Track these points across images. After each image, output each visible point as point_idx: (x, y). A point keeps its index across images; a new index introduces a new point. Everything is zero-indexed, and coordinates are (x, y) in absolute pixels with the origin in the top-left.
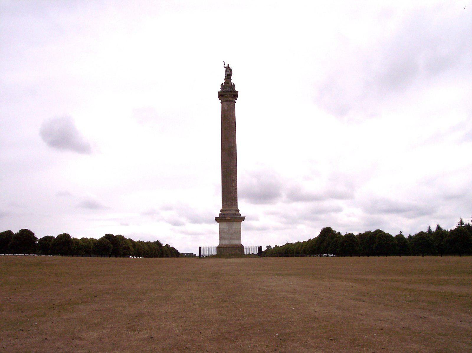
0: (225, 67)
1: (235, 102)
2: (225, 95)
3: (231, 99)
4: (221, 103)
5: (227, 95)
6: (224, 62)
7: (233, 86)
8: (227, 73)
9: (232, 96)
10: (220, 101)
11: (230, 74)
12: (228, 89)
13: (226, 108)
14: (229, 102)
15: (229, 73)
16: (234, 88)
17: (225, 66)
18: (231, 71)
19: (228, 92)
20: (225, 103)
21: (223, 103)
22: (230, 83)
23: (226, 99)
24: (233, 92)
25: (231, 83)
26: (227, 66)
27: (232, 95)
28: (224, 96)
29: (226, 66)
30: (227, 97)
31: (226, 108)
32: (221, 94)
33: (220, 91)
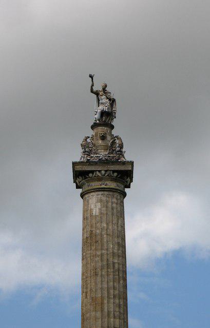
0: (97, 94)
1: (124, 195)
2: (92, 172)
3: (112, 185)
4: (82, 196)
5: (100, 171)
6: (91, 77)
7: (116, 148)
8: (101, 107)
9: (116, 174)
10: (80, 191)
11: (110, 111)
12: (102, 154)
13: (96, 211)
14: (106, 193)
15: (106, 109)
16: (121, 153)
17: (95, 89)
18: (113, 102)
19: (102, 162)
20: (93, 198)
21: (86, 196)
22: (109, 138)
23: (96, 185)
24: (117, 162)
25: (114, 138)
26: (101, 89)
27: (114, 171)
28: (91, 175)
29: (98, 87)
30: (99, 179)
31: (96, 211)
32: (79, 168)
33: (77, 159)
